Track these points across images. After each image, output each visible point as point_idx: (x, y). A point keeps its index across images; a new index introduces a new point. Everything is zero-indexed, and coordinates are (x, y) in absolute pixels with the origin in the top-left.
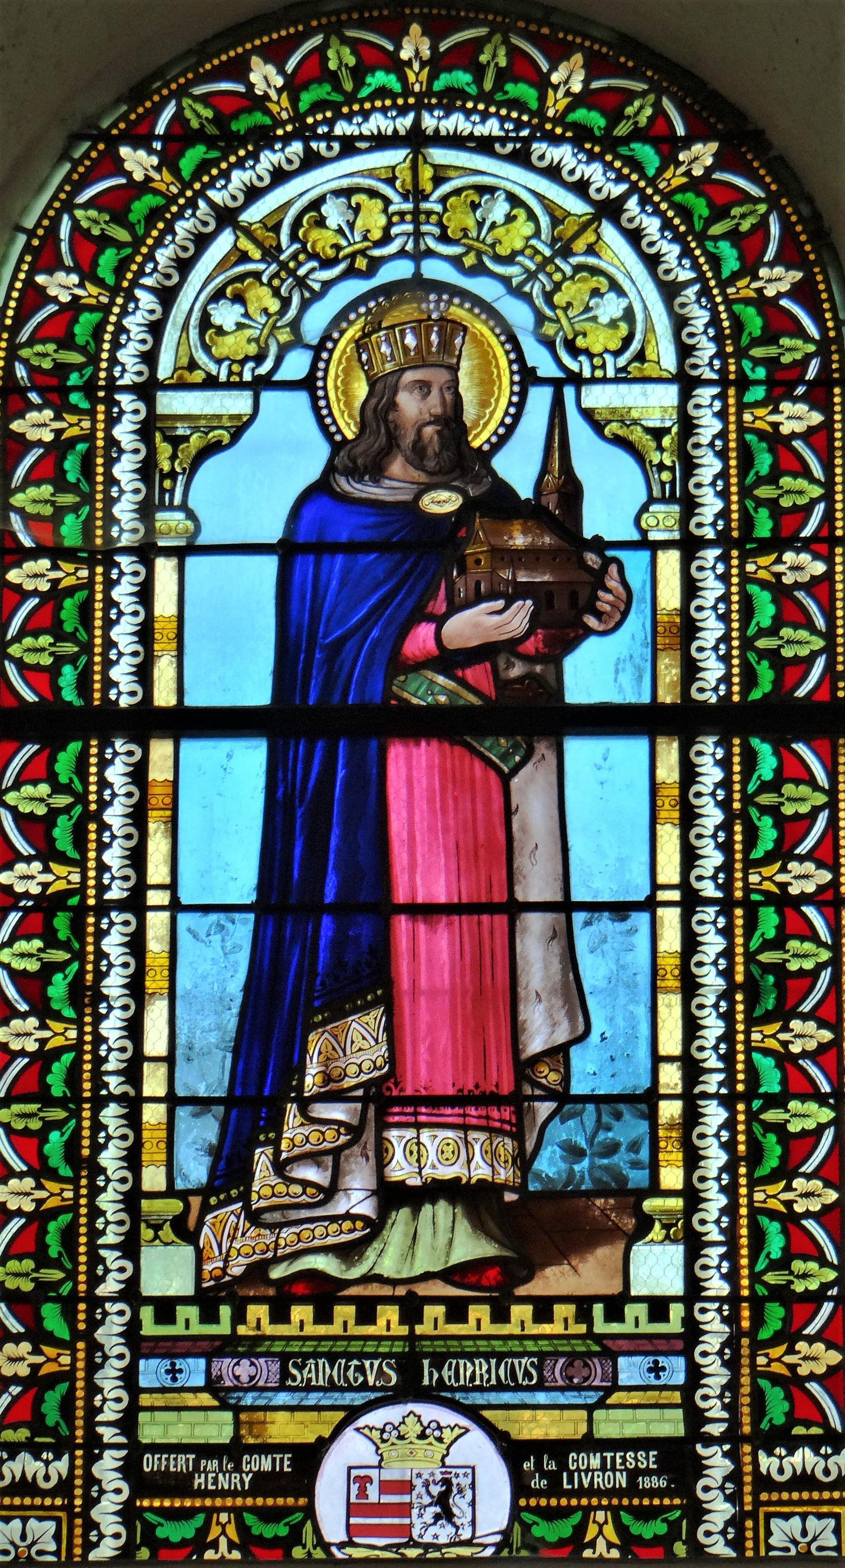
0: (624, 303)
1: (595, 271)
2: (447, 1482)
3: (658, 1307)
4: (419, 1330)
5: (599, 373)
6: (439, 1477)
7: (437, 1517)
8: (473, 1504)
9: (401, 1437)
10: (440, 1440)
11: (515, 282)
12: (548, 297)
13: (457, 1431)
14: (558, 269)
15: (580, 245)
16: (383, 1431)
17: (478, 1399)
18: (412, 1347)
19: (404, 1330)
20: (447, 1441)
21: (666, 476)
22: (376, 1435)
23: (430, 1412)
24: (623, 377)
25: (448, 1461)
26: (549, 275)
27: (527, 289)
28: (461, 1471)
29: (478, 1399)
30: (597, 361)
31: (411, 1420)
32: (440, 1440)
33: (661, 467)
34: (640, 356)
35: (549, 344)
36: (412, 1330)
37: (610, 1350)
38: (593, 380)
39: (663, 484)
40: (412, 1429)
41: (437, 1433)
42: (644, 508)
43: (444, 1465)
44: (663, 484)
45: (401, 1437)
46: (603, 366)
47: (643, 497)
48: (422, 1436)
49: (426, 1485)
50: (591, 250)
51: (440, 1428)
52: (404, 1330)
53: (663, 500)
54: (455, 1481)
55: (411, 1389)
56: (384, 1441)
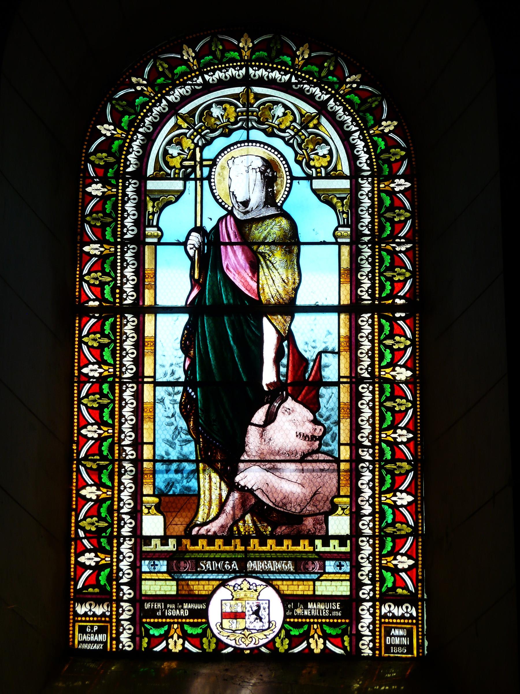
0: (329, 148)
1: (317, 135)
2: (259, 606)
3: (342, 540)
5: (319, 175)
8: (269, 614)
10: (256, 591)
11: (286, 139)
12: (299, 146)
14: (303, 134)
15: (311, 125)
16: (234, 587)
17: (272, 577)
18: (246, 555)
19: (243, 548)
20: (259, 591)
21: (345, 216)
22: (231, 588)
24: (328, 177)
25: (259, 598)
26: (300, 136)
27: (291, 141)
28: (264, 602)
29: (272, 577)
32: (256, 591)
33: (343, 212)
34: (335, 169)
36: (246, 548)
37: (323, 557)
38: (317, 178)
40: (245, 586)
42: (336, 229)
43: (258, 600)
44: (344, 219)
45: (241, 589)
46: (321, 172)
48: (249, 589)
52: (243, 548)
53: (344, 226)
54: (262, 606)
56: (235, 591)
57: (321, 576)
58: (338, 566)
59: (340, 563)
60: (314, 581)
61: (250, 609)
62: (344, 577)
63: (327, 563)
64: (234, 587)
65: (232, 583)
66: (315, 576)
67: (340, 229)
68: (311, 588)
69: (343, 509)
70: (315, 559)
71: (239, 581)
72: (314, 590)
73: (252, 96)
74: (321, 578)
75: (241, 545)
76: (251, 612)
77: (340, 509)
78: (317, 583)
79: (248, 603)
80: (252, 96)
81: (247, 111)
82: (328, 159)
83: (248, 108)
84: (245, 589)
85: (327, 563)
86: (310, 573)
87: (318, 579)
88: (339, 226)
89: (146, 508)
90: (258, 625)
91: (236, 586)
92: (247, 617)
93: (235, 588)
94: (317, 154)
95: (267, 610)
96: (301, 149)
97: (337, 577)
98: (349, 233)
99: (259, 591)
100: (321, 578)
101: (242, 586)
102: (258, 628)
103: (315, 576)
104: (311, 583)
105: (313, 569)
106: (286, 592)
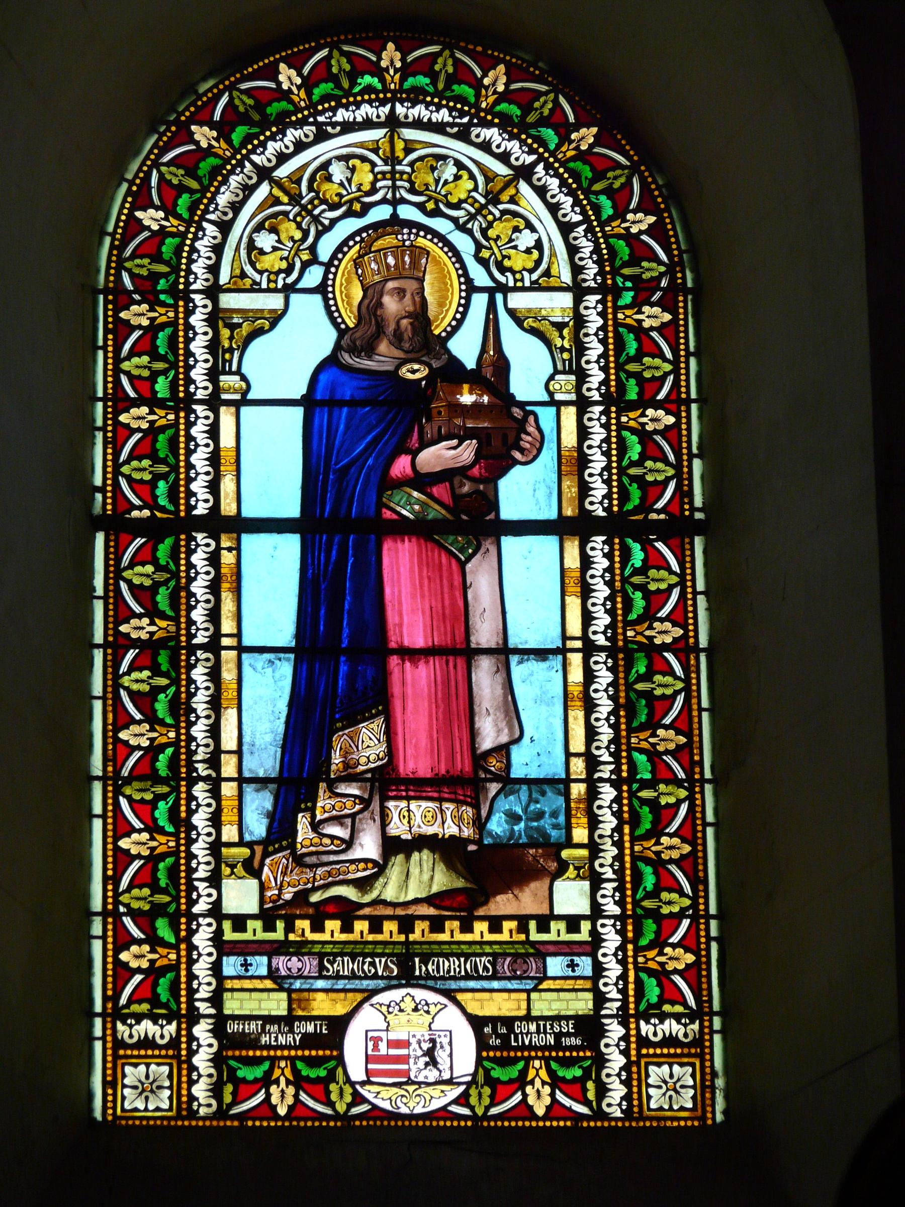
0: (535, 236)
1: (515, 214)
2: (433, 1041)
4: (412, 937)
5: (519, 284)
6: (427, 1037)
7: (427, 1064)
8: (451, 1055)
9: (401, 1010)
10: (428, 1012)
11: (461, 221)
12: (484, 232)
13: (439, 1007)
14: (491, 213)
15: (505, 197)
16: (389, 1006)
18: (407, 949)
19: (402, 938)
20: (433, 1013)
21: (566, 356)
22: (384, 1009)
23: (420, 994)
24: (536, 287)
25: (433, 1027)
26: (485, 217)
27: (469, 226)
28: (442, 1034)
30: (518, 276)
31: (408, 999)
32: (428, 1012)
33: (563, 349)
34: (547, 273)
35: (484, 263)
36: (407, 937)
38: (515, 289)
39: (564, 361)
40: (408, 1005)
41: (426, 1008)
42: (551, 378)
44: (564, 361)
45: (401, 1010)
46: (522, 280)
47: (551, 371)
48: (416, 1010)
49: (419, 1042)
50: (513, 200)
51: (427, 1004)
52: (402, 938)
53: (564, 372)
54: (438, 1040)
55: (407, 978)
56: (389, 1013)
57: (540, 983)
58: (568, 966)
59: (572, 961)
60: (528, 992)
61: (417, 1046)
62: (580, 984)
63: (549, 960)
64: (389, 1006)
65: (384, 998)
66: (530, 985)
67: (557, 377)
68: (524, 1005)
69: (577, 868)
70: (528, 955)
71: (395, 995)
72: (529, 1009)
73: (400, 145)
74: (541, 987)
75: (400, 932)
76: (420, 1053)
77: (571, 867)
78: (534, 995)
79: (414, 1036)
80: (400, 145)
81: (393, 172)
82: (535, 254)
83: (393, 167)
84: (409, 1010)
85: (549, 960)
86: (520, 978)
87: (535, 989)
88: (556, 372)
89: (227, 865)
90: (432, 1075)
91: (393, 1004)
92: (412, 1061)
93: (391, 1010)
94: (515, 247)
95: (448, 1048)
96: (487, 239)
97: (569, 984)
98: (574, 383)
99: (433, 1012)
100: (541, 987)
101: (403, 1005)
102: (431, 1080)
103: (530, 985)
104: (524, 996)
105: (525, 972)
106: (480, 1013)
